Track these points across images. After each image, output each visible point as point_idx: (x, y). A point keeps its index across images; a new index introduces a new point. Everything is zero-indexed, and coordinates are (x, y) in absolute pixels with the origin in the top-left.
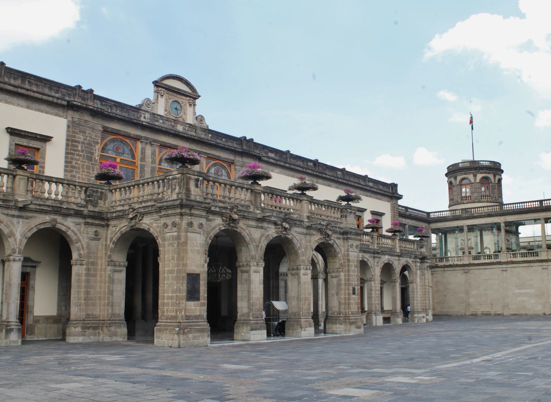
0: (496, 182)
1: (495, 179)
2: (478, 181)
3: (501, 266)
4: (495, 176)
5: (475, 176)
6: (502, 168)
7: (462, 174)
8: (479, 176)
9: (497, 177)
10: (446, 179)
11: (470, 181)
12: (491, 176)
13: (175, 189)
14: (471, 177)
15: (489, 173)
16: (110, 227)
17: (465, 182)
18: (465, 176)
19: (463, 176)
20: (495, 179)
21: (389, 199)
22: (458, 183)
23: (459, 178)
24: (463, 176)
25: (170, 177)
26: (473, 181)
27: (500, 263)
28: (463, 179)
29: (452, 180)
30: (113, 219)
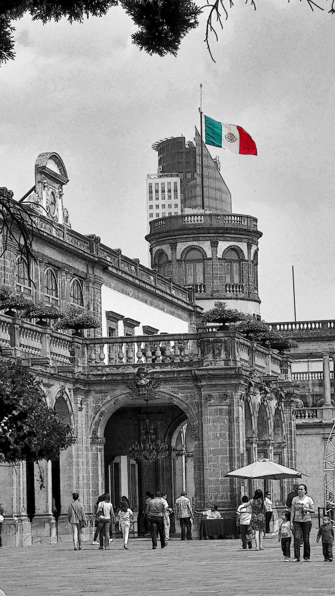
0: (252, 259)
1: (249, 253)
2: (220, 255)
3: (321, 431)
4: (249, 247)
5: (214, 245)
6: (259, 229)
7: (187, 240)
8: (223, 246)
9: (254, 248)
10: (147, 244)
11: (204, 253)
12: (243, 246)
13: (220, 354)
14: (206, 246)
15: (240, 240)
16: (93, 393)
17: (195, 255)
18: (195, 243)
19: (190, 244)
20: (249, 253)
21: (185, 315)
22: (179, 257)
23: (181, 247)
24: (190, 244)
25: (211, 339)
26: (209, 255)
27: (320, 425)
28: (192, 248)
29: (166, 248)
30: (99, 383)
